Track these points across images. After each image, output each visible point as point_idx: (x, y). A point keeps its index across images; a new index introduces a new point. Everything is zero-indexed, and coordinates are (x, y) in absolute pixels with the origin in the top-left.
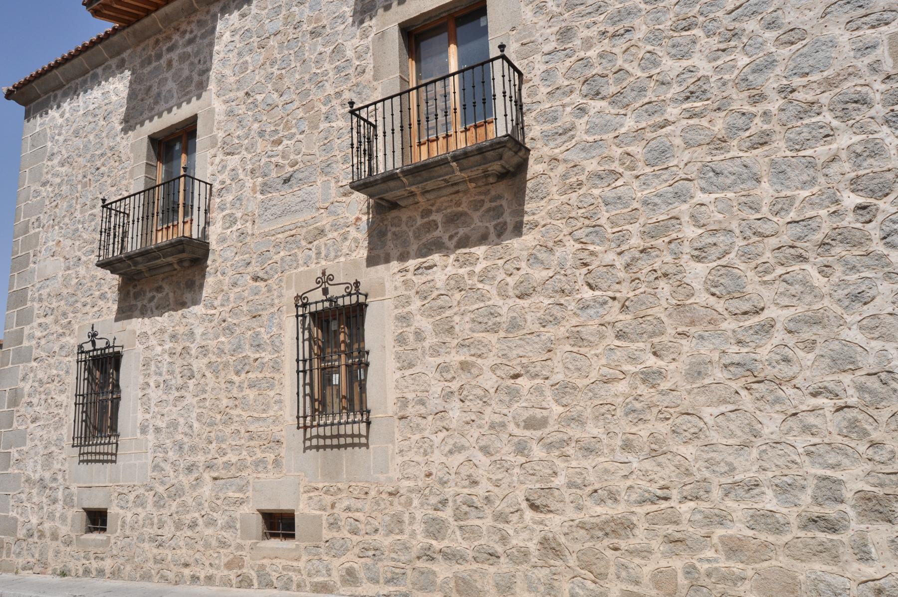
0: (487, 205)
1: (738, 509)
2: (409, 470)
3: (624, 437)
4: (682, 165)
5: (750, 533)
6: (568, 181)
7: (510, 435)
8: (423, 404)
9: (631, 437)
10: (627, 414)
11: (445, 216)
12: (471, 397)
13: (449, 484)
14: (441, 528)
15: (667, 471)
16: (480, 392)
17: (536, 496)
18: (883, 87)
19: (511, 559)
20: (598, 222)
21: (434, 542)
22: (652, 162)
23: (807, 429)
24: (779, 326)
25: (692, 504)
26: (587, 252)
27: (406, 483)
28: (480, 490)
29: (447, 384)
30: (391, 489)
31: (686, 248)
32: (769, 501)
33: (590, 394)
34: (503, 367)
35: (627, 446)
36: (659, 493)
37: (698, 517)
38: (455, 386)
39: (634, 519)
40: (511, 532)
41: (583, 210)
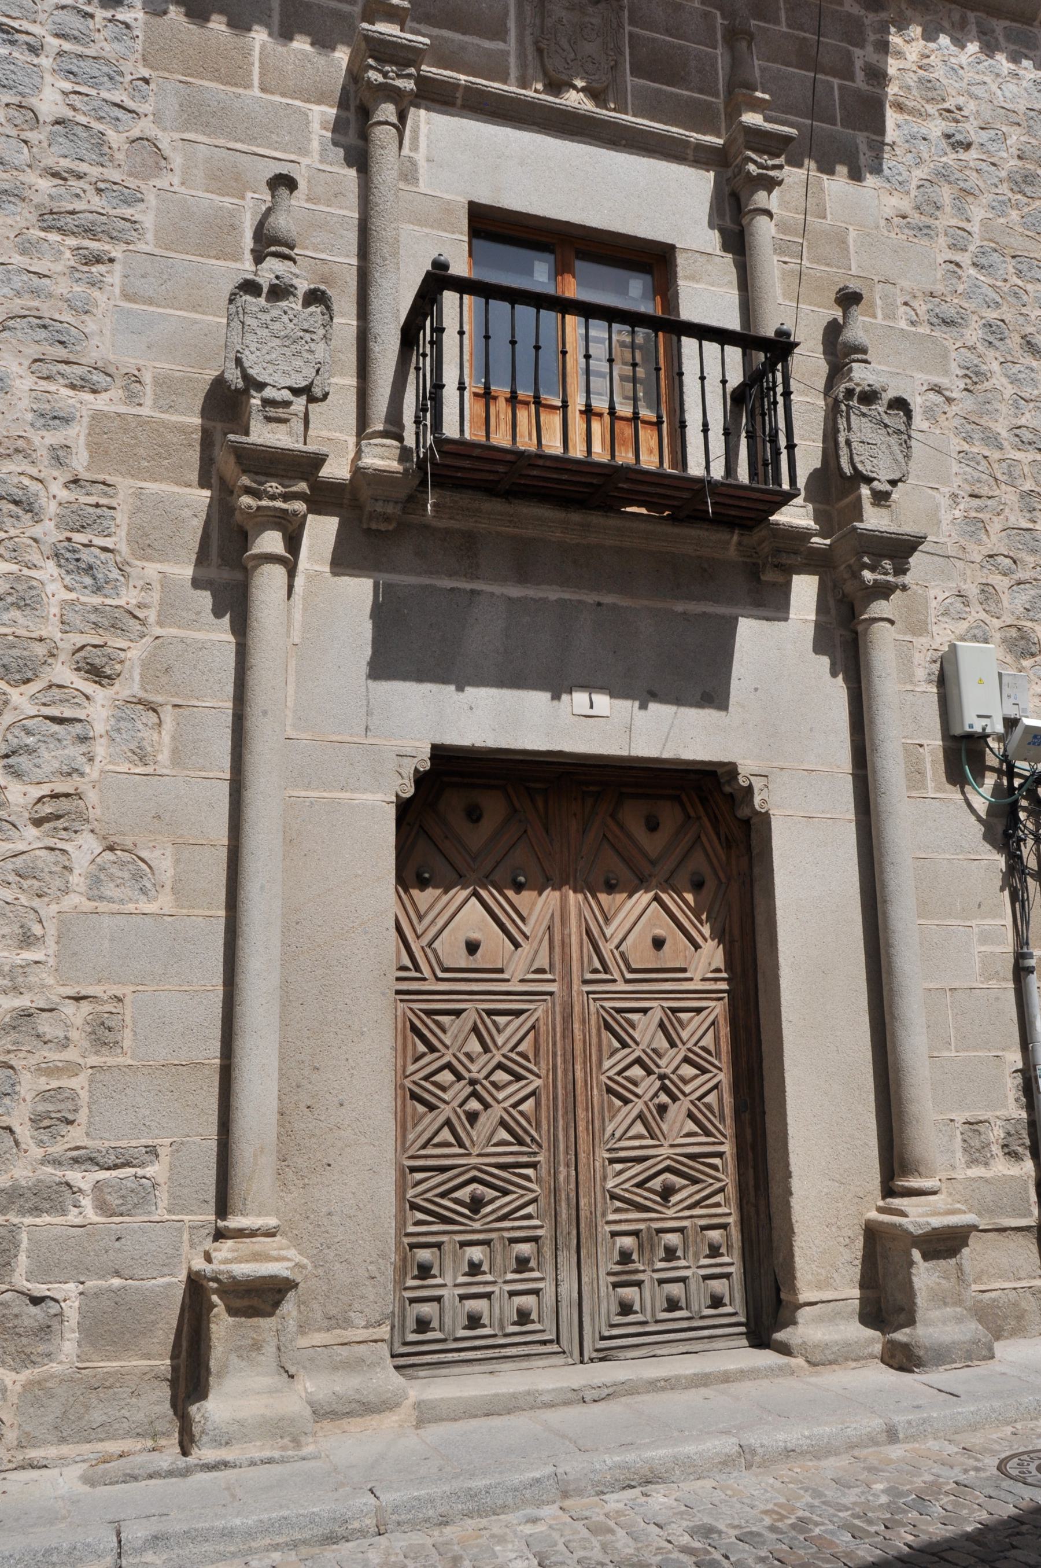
18: (64, 494)
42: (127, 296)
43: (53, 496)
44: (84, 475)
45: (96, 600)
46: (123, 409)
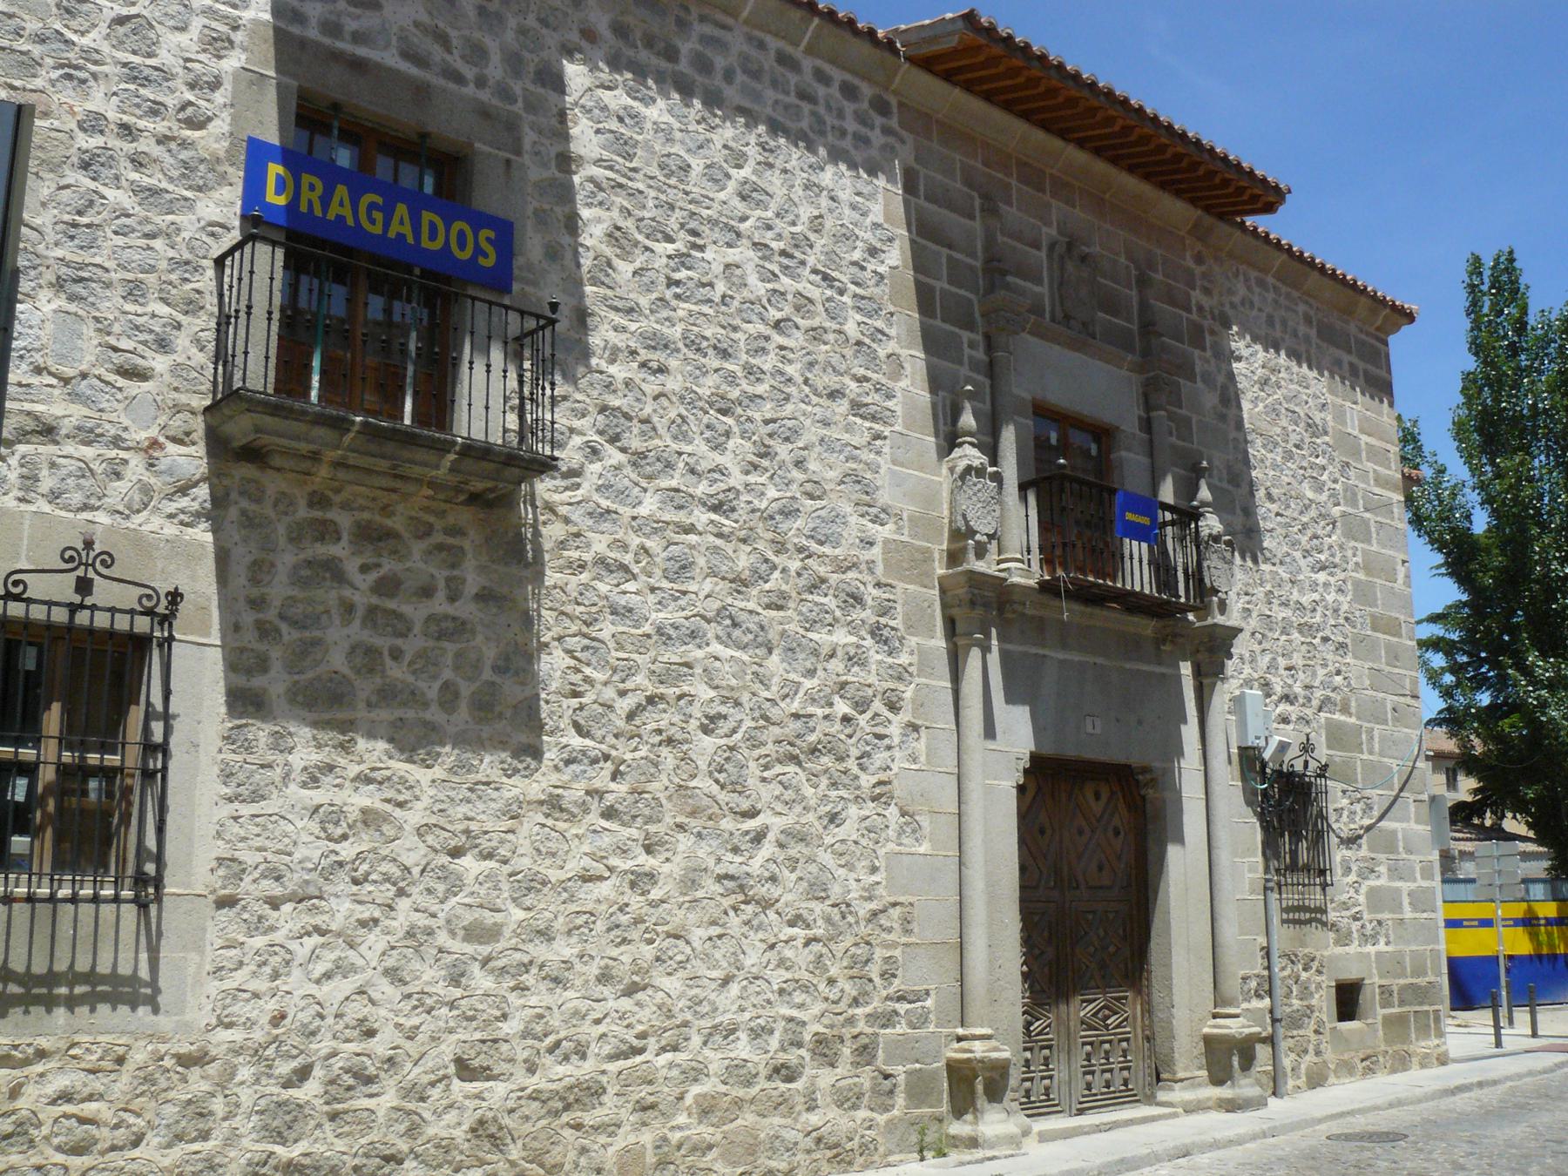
0: (438, 538)
1: (715, 1060)
2: (234, 1009)
3: (602, 963)
4: (701, 596)
5: (723, 1088)
6: (566, 553)
7: (440, 951)
8: (278, 879)
9: (611, 962)
10: (609, 930)
11: (358, 524)
12: (373, 877)
13: (318, 1038)
14: (295, 1120)
15: (647, 1011)
16: (395, 871)
17: (473, 1053)
19: (423, 1162)
20: (600, 635)
21: (278, 1149)
22: (671, 575)
23: (782, 963)
24: (771, 836)
25: (669, 1056)
26: (579, 676)
27: (224, 1035)
28: (379, 1046)
29: (332, 846)
30: (185, 1049)
31: (696, 711)
32: (743, 1048)
33: (565, 895)
34: (438, 831)
35: (604, 977)
36: (635, 1042)
37: (675, 1073)
38: (347, 851)
39: (604, 1079)
40: (427, 1115)
41: (582, 609)
42: (894, 462)
43: (871, 593)
44: (884, 580)
45: (890, 660)
46: (896, 537)
